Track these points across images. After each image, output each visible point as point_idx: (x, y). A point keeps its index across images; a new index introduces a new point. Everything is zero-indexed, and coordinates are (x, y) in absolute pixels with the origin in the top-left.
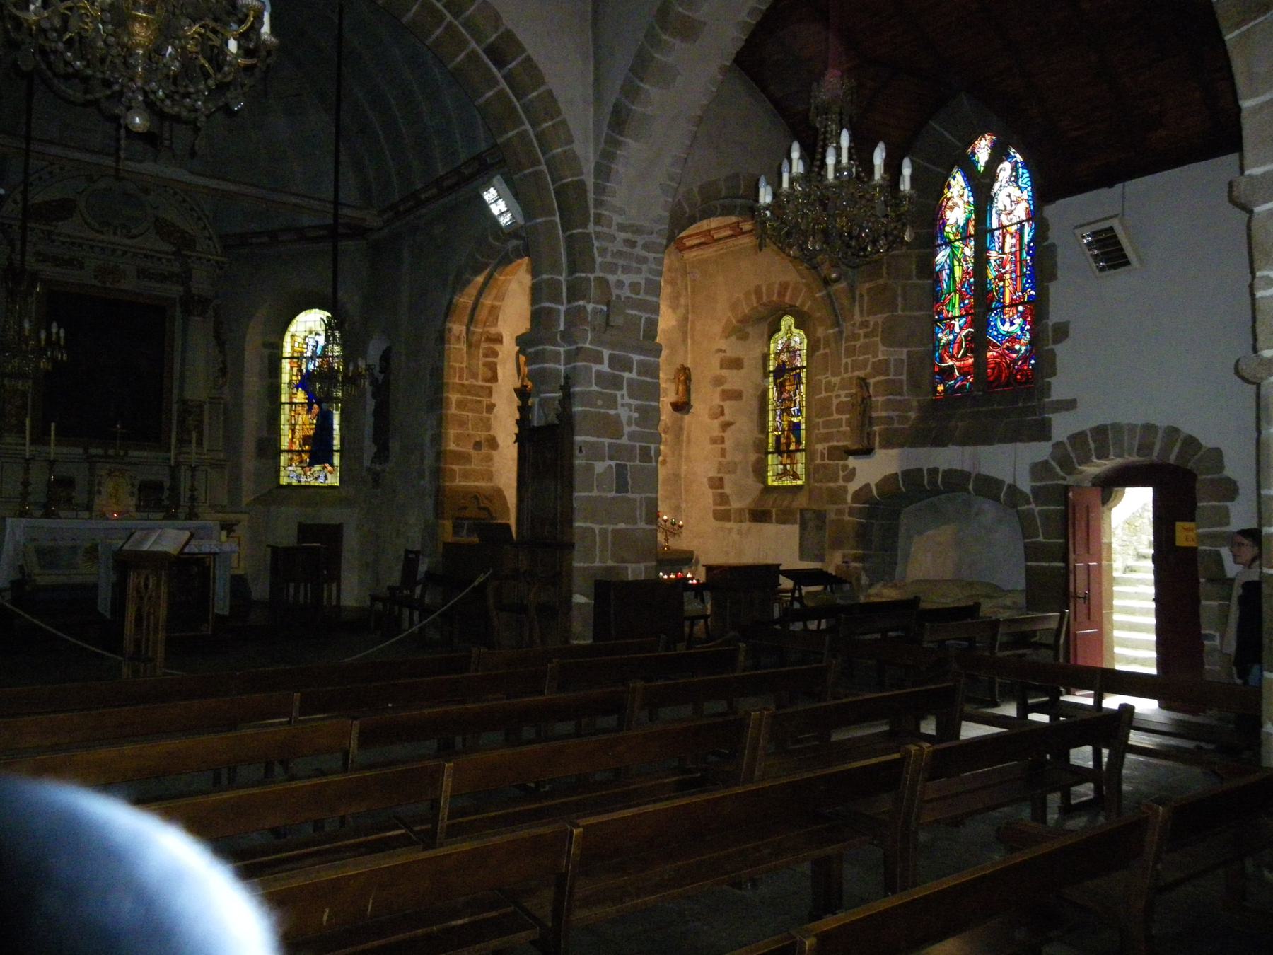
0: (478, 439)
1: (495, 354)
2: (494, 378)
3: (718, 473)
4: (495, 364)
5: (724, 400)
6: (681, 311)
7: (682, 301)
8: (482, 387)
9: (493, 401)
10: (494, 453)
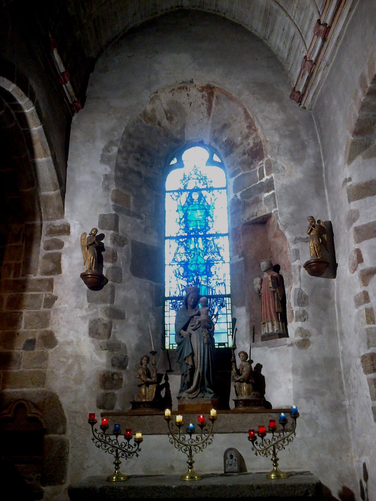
0: (30, 338)
1: (60, 245)
2: (58, 269)
3: (369, 347)
4: (60, 255)
5: (358, 241)
6: (310, 162)
7: (310, 151)
8: (40, 281)
9: (54, 294)
10: (50, 351)
